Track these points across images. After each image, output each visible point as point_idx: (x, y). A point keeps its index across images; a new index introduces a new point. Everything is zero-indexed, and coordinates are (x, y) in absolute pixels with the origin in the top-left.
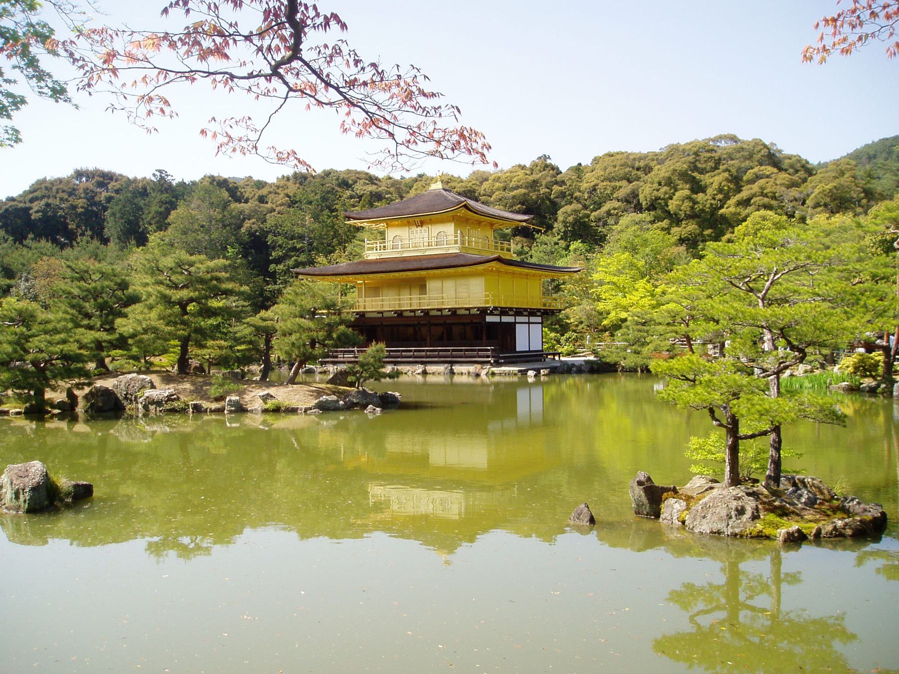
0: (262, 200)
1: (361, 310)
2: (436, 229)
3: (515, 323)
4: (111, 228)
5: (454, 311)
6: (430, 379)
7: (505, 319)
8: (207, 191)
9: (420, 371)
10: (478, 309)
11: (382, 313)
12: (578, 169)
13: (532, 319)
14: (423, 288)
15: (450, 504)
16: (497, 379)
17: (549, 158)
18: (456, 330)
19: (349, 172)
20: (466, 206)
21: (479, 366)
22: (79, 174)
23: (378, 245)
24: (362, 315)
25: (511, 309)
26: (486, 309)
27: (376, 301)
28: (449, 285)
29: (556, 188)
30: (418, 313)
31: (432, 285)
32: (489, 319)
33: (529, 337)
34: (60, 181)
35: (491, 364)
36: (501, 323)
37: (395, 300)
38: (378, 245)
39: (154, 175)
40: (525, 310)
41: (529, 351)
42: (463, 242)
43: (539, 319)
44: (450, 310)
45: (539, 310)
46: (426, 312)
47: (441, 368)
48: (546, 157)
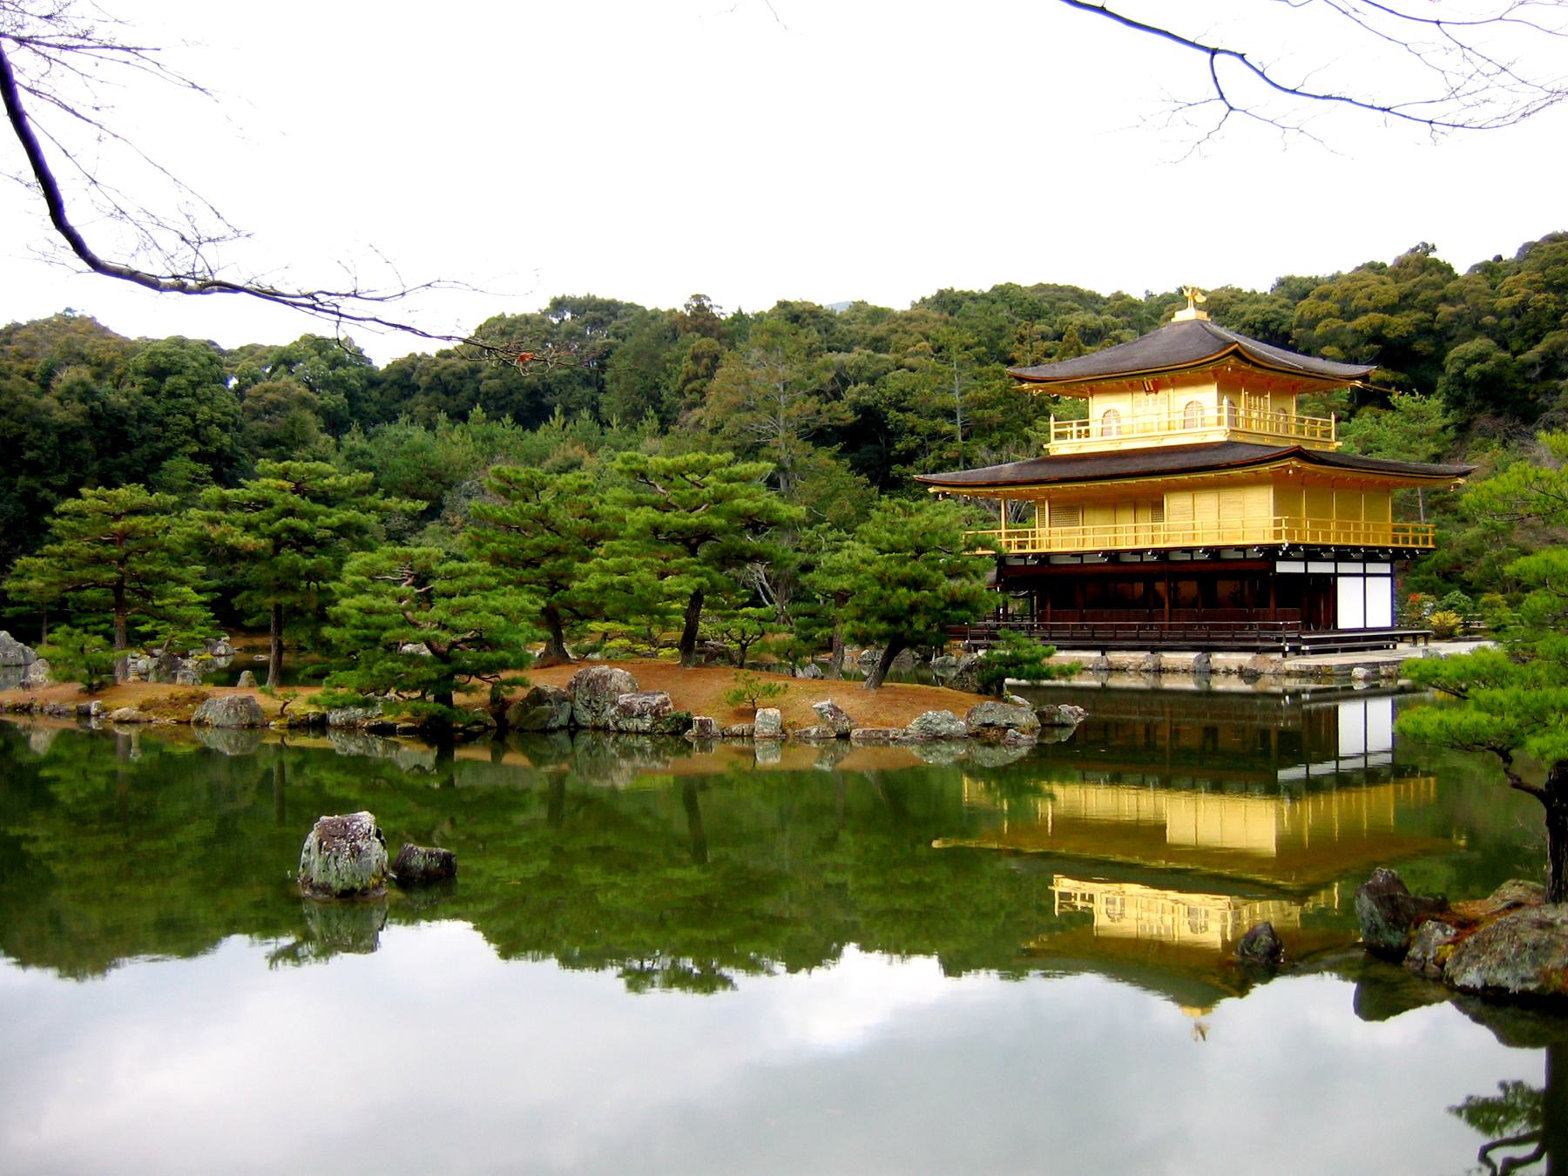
0: (878, 344)
1: (1044, 550)
3: (1336, 575)
4: (611, 402)
6: (1169, 683)
7: (1316, 568)
8: (775, 333)
9: (1149, 665)
10: (1261, 548)
12: (1491, 270)
13: (1372, 568)
14: (1157, 507)
15: (1205, 920)
16: (1292, 684)
17: (1434, 249)
18: (1224, 588)
19: (1041, 288)
20: (1236, 353)
22: (559, 305)
23: (1075, 429)
24: (1044, 558)
25: (1326, 548)
26: (1279, 547)
27: (1070, 533)
28: (1207, 503)
29: (1444, 310)
30: (1149, 557)
31: (1175, 504)
32: (1282, 567)
33: (1364, 601)
34: (526, 320)
35: (1285, 655)
37: (1106, 531)
38: (1075, 429)
39: (687, 306)
40: (1356, 549)
41: (1365, 629)
42: (1234, 421)
43: (1386, 568)
44: (1207, 549)
45: (1384, 550)
46: (1163, 554)
47: (1190, 657)
48: (1428, 248)
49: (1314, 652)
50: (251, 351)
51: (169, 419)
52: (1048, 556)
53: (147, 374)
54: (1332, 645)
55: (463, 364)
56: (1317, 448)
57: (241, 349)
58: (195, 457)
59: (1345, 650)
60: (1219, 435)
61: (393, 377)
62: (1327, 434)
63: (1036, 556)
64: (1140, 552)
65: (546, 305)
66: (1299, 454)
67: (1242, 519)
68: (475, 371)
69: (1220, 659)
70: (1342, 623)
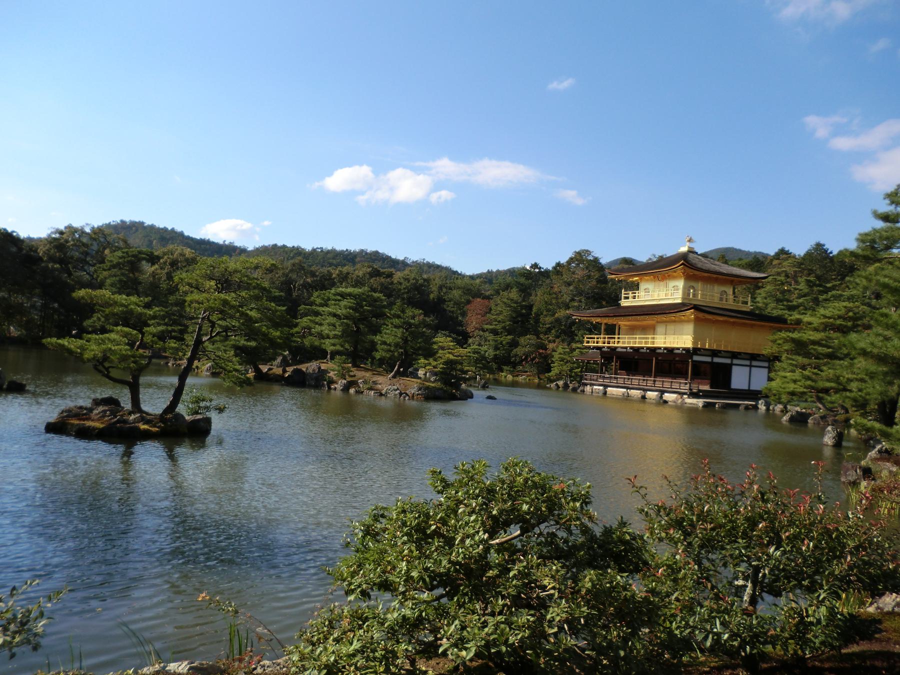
2: (672, 284)
3: (731, 365)
5: (670, 350)
7: (716, 360)
10: (684, 349)
11: (626, 348)
13: (754, 363)
24: (614, 349)
25: (720, 351)
32: (696, 358)
36: (712, 363)
38: (631, 295)
40: (740, 353)
41: (749, 390)
43: (766, 364)
44: (665, 348)
46: (653, 350)
52: (616, 348)
60: (679, 301)
62: (746, 303)
63: (608, 347)
64: (643, 348)
66: (696, 308)
67: (679, 338)
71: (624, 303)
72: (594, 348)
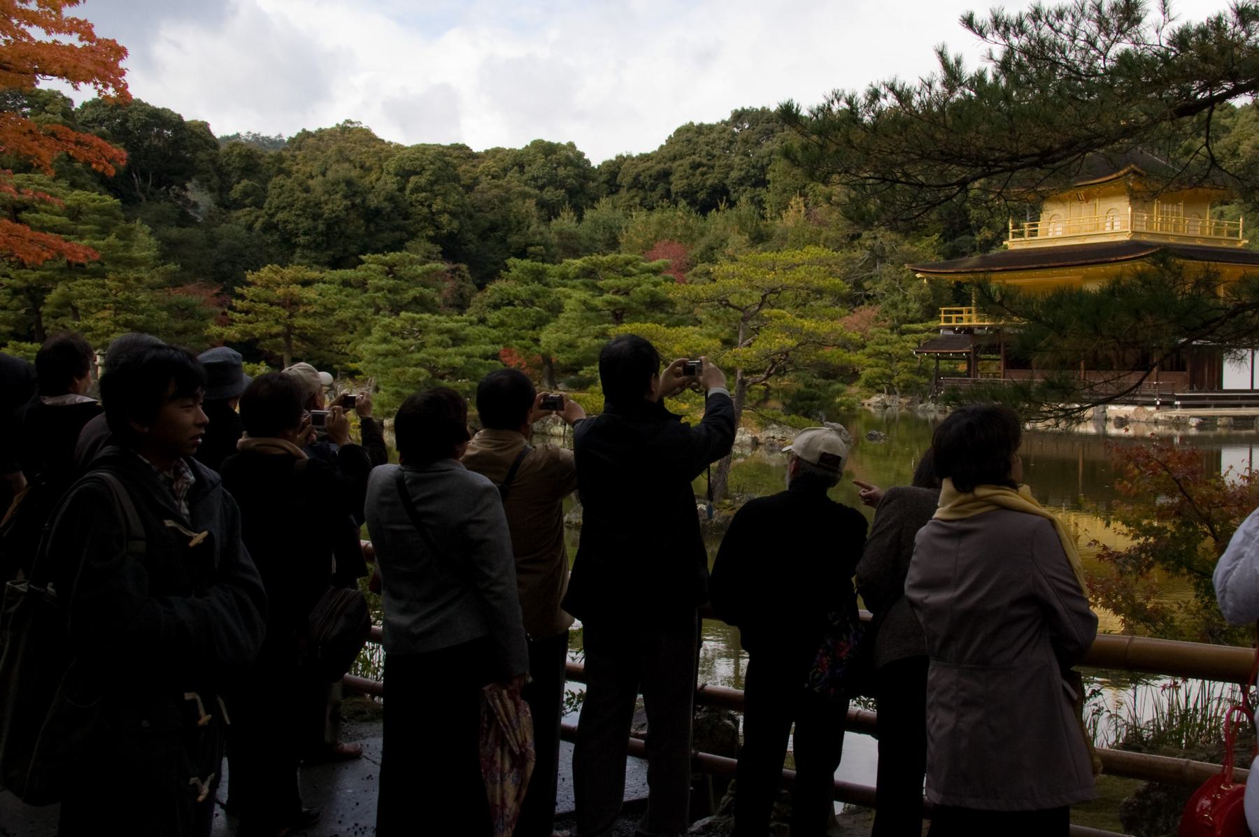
2: (1103, 206)
21: (1140, 410)
34: (711, 128)
35: (1158, 407)
41: (1252, 390)
49: (1183, 406)
50: (495, 153)
51: (412, 210)
53: (396, 175)
54: (1207, 402)
55: (658, 167)
56: (1224, 245)
57: (487, 152)
58: (432, 240)
59: (1217, 406)
61: (602, 179)
62: (1237, 234)
65: (727, 117)
68: (665, 175)
69: (1114, 410)
70: (1226, 386)
71: (1013, 244)
72: (962, 328)
